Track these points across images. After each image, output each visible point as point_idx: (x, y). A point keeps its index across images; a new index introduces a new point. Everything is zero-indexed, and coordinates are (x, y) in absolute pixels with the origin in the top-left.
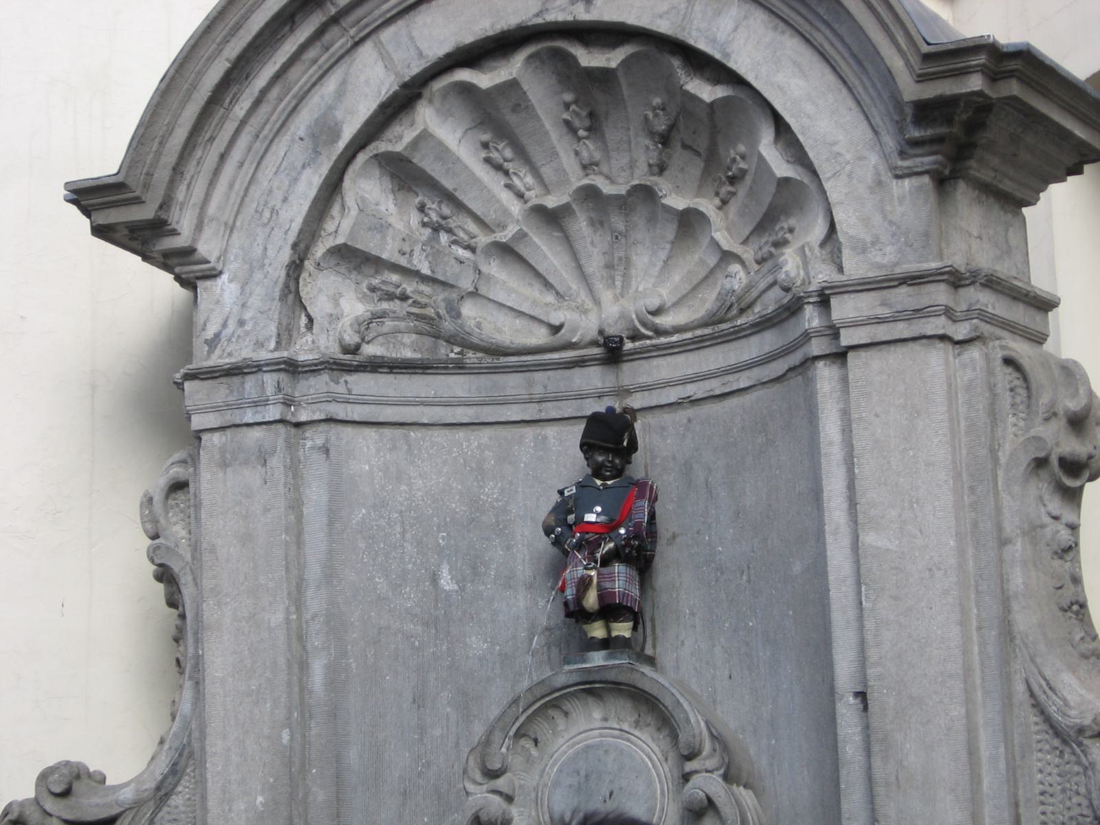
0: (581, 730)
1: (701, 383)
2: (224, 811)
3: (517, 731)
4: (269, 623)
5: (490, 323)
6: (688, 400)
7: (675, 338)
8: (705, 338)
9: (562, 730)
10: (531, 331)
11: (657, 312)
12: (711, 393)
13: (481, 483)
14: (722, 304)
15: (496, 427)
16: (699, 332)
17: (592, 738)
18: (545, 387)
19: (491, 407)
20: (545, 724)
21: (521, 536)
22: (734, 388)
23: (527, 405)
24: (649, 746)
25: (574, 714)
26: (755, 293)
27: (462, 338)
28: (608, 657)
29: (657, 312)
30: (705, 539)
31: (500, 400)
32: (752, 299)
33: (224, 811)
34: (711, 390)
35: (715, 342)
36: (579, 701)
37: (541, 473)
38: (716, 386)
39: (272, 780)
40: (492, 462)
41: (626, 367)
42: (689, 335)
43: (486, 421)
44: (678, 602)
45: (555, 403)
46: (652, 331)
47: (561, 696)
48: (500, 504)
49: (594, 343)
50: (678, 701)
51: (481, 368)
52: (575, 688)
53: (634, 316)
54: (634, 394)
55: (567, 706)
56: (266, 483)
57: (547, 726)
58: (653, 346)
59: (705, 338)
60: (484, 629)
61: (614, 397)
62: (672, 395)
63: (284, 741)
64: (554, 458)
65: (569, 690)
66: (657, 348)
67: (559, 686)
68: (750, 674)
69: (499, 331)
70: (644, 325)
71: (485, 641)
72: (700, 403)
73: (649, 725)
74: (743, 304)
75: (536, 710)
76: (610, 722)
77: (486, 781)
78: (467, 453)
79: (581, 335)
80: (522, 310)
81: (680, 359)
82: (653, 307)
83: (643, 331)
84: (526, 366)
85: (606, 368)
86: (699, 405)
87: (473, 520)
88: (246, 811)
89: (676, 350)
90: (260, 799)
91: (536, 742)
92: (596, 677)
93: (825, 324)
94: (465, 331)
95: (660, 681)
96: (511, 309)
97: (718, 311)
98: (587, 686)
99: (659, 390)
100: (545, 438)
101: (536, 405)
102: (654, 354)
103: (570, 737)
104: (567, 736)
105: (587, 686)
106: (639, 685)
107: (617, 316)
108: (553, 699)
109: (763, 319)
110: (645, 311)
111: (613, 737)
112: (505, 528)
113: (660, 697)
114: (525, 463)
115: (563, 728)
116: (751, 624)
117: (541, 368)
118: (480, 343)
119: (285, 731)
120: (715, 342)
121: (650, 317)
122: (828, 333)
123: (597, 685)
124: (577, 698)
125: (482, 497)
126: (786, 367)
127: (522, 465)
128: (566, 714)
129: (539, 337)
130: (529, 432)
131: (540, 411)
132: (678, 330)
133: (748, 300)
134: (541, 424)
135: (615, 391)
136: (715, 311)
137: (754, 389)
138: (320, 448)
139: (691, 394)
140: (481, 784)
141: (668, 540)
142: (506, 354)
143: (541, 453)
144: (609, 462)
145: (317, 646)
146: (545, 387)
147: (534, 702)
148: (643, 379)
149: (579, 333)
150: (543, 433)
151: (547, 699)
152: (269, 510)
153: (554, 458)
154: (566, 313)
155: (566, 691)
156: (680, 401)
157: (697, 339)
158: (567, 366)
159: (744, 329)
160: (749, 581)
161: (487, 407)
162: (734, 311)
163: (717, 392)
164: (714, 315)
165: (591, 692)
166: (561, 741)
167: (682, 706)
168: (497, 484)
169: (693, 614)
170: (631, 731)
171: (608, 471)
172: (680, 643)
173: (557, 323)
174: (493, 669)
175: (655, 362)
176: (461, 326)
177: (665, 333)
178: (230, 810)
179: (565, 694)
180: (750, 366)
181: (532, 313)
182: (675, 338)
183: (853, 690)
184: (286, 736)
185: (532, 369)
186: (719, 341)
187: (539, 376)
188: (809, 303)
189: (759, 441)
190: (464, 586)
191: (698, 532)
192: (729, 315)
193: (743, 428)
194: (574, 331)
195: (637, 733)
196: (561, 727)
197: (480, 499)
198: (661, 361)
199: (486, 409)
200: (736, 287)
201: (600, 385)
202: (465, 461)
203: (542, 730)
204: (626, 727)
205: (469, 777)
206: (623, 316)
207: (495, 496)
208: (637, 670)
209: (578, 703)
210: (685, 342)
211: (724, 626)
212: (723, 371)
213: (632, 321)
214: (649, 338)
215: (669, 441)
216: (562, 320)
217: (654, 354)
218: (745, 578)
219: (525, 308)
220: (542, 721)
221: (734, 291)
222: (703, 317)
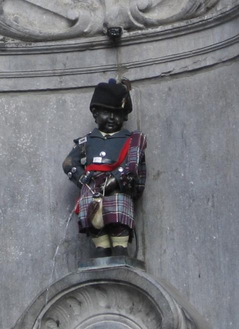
0: (91, 314)
1: (178, 62)
3: (44, 315)
5: (24, 18)
6: (169, 74)
7: (159, 29)
8: (181, 29)
9: (77, 315)
10: (54, 24)
11: (146, 10)
13: (18, 135)
14: (194, 4)
15: (29, 94)
16: (176, 25)
17: (99, 321)
18: (65, 65)
19: (25, 79)
20: (64, 310)
21: (47, 173)
22: (203, 65)
23: (52, 78)
25: (86, 303)
27: (4, 29)
28: (111, 262)
29: (146, 10)
30: (181, 175)
31: (32, 74)
34: (186, 67)
35: (188, 32)
36: (89, 294)
37: (62, 128)
38: (189, 64)
40: (26, 119)
41: (124, 50)
42: (169, 27)
43: (22, 89)
44: (162, 221)
45: (72, 76)
46: (142, 24)
47: (76, 290)
48: (32, 150)
49: (100, 33)
50: (161, 294)
51: (17, 51)
52: (87, 284)
53: (129, 13)
54: (129, 70)
55: (81, 297)
57: (66, 312)
58: (143, 35)
59: (181, 29)
60: (20, 241)
61: (115, 72)
62: (157, 71)
65: (82, 286)
66: (146, 36)
67: (74, 282)
68: (214, 274)
69: (31, 24)
70: (137, 19)
71: (21, 250)
72: (177, 76)
73: (140, 311)
74: (209, 4)
75: (57, 300)
76: (111, 309)
78: (7, 113)
79: (91, 27)
80: (47, 8)
81: (163, 44)
82: (143, 7)
83: (136, 23)
84: (51, 49)
86: (177, 78)
87: (12, 162)
89: (160, 38)
91: (58, 323)
92: (102, 276)
94: (6, 24)
95: (148, 279)
96: (40, 7)
97: (190, 9)
98: (95, 283)
100: (65, 102)
101: (58, 78)
103: (83, 319)
104: (80, 319)
105: (95, 283)
106: (133, 282)
107: (117, 13)
108: (70, 292)
109: (223, 15)
110: (137, 9)
111: (115, 320)
112: (35, 167)
113: (148, 291)
114: (50, 120)
115: (78, 314)
116: (215, 238)
117: (62, 51)
118: (17, 32)
120: (188, 32)
121: (141, 13)
123: (103, 282)
124: (88, 291)
125: (19, 145)
127: (48, 122)
128: (80, 303)
129: (60, 28)
130: (53, 97)
131: (61, 82)
132: (162, 23)
134: (61, 91)
135: (116, 68)
136: (188, 9)
139: (171, 70)
141: (154, 176)
142: (36, 41)
143: (62, 113)
144: (111, 119)
146: (65, 65)
147: (57, 295)
148: (136, 59)
149: (89, 26)
150: (63, 98)
151: (66, 292)
153: (71, 116)
154: (79, 10)
155: (79, 286)
156: (162, 75)
157: (175, 30)
158: (80, 49)
159: (210, 23)
160: (213, 206)
161: (22, 79)
162: (202, 10)
163: (190, 68)
164: (187, 12)
165: (98, 287)
166: (76, 323)
167: (164, 297)
168: (30, 135)
169: (172, 230)
170: (127, 315)
171: (110, 126)
172: (163, 251)
173: (73, 18)
174: (27, 271)
175: (145, 46)
176: (4, 20)
177: (152, 25)
179: (79, 288)
181: (55, 11)
182: (159, 29)
185: (55, 51)
186: (191, 31)
187: (60, 57)
189: (221, 104)
190: (6, 210)
191: (176, 171)
192: (199, 12)
193: (209, 95)
194: (86, 23)
195: (131, 317)
196: (76, 313)
197: (17, 146)
198: (149, 46)
199: (22, 81)
201: (104, 63)
202: (6, 118)
203: (62, 315)
204: (123, 313)
206: (121, 13)
207: (28, 144)
208: (131, 271)
209: (88, 295)
210: (167, 32)
211: (195, 239)
213: (128, 16)
214: (140, 29)
215: (155, 104)
216: (77, 16)
218: (210, 204)
219: (49, 7)
220: (62, 309)
222: (180, 14)
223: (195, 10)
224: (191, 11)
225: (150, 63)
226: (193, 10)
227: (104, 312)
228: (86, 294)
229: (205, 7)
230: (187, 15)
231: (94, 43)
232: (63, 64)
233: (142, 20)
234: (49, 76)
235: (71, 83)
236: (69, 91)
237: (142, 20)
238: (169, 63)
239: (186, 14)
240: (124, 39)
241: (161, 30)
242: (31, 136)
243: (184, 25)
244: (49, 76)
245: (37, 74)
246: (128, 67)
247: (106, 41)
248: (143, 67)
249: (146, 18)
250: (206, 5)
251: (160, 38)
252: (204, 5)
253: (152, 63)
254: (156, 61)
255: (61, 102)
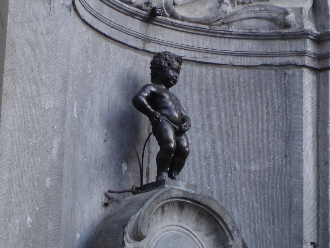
2: (5, 221)
4: (45, 105)
7: (185, 23)
8: (203, 30)
12: (195, 59)
14: (217, 17)
16: (201, 26)
18: (117, 21)
24: (200, 243)
25: (167, 214)
26: (236, 18)
32: (233, 20)
33: (5, 221)
34: (196, 58)
36: (173, 207)
38: (200, 57)
39: (38, 208)
41: (151, 27)
42: (194, 25)
45: (117, 31)
52: (178, 200)
54: (151, 43)
56: (49, 15)
58: (171, 22)
63: (47, 185)
64: (112, 61)
66: (173, 24)
73: (201, 231)
77: (132, 241)
81: (182, 35)
85: (142, 23)
88: (20, 224)
89: (181, 29)
90: (29, 219)
93: (313, 51)
97: (211, 19)
99: (164, 46)
102: (169, 26)
106: (213, 208)
119: (48, 179)
122: (313, 56)
123: (188, 201)
126: (261, 63)
132: (183, 19)
133: (230, 20)
136: (210, 18)
137: (225, 66)
138: (67, 7)
139: (183, 55)
140: (129, 242)
145: (56, 129)
148: (160, 38)
152: (50, 33)
157: (197, 28)
159: (231, 34)
162: (219, 23)
163: (199, 60)
164: (208, 20)
175: (167, 31)
178: (9, 221)
180: (226, 54)
182: (185, 23)
183: (311, 241)
184: (48, 182)
186: (210, 34)
188: (309, 38)
192: (215, 23)
196: (159, 220)
200: (228, 11)
201: (138, 31)
205: (126, 237)
210: (190, 28)
212: (205, 50)
213: (163, 4)
217: (169, 26)
221: (226, 12)
222: (202, 18)
223: (215, 20)
224: (211, 20)
225: (168, 45)
226: (213, 20)
227: (177, 224)
228: (171, 207)
229: (222, 22)
230: (206, 21)
231: (138, 13)
232: (116, 19)
233: (172, 11)
234: (106, 24)
235: (116, 36)
236: (112, 41)
237: (172, 11)
238: (181, 50)
239: (206, 20)
240: (157, 20)
241: (186, 25)
242: (92, 65)
243: (206, 28)
244: (106, 24)
245: (103, 19)
246: (151, 41)
247: (146, 16)
248: (161, 45)
249: (175, 12)
250: (223, 20)
251: (181, 29)
252: (223, 19)
253: (170, 45)
254: (173, 45)
255: (107, 47)
